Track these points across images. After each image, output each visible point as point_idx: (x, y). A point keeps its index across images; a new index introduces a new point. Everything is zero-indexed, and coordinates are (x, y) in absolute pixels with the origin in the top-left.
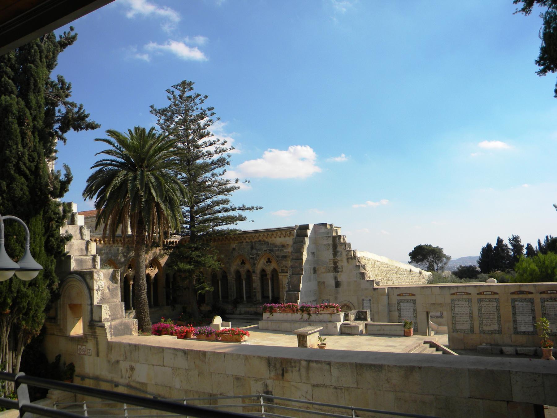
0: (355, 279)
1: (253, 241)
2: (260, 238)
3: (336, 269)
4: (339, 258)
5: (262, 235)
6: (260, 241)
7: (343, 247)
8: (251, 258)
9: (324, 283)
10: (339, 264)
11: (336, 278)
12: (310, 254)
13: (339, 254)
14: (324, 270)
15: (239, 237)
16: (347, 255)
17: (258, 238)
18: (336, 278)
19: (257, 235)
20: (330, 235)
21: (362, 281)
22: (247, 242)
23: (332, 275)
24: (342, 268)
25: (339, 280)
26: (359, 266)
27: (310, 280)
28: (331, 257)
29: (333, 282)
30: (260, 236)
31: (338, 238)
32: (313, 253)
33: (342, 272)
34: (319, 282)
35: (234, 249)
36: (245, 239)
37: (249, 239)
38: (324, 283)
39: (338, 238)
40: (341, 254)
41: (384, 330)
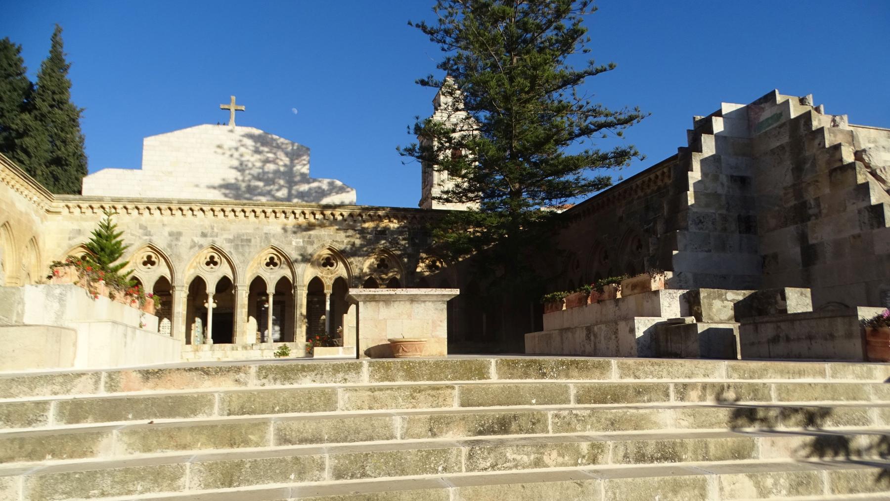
0: (857, 231)
1: (649, 191)
2: (660, 183)
3: (801, 214)
4: (808, 177)
5: (659, 173)
6: (659, 188)
7: (817, 142)
8: (647, 231)
9: (775, 256)
10: (810, 196)
11: (803, 238)
12: (723, 178)
13: (808, 166)
14: (773, 222)
15: (625, 192)
16: (828, 163)
17: (655, 182)
18: (803, 238)
19: (652, 176)
20: (783, 120)
21: (881, 229)
22: (639, 198)
23: (791, 230)
24: (818, 205)
25: (812, 241)
26: (866, 186)
27: (722, 247)
28: (789, 179)
29: (795, 251)
30: (657, 177)
31: (802, 122)
32: (742, 181)
33: (816, 216)
34: (764, 258)
35: (621, 219)
36: (636, 192)
37: (642, 189)
38: (775, 256)
39: (802, 122)
40: (814, 164)
41: (788, 339)
